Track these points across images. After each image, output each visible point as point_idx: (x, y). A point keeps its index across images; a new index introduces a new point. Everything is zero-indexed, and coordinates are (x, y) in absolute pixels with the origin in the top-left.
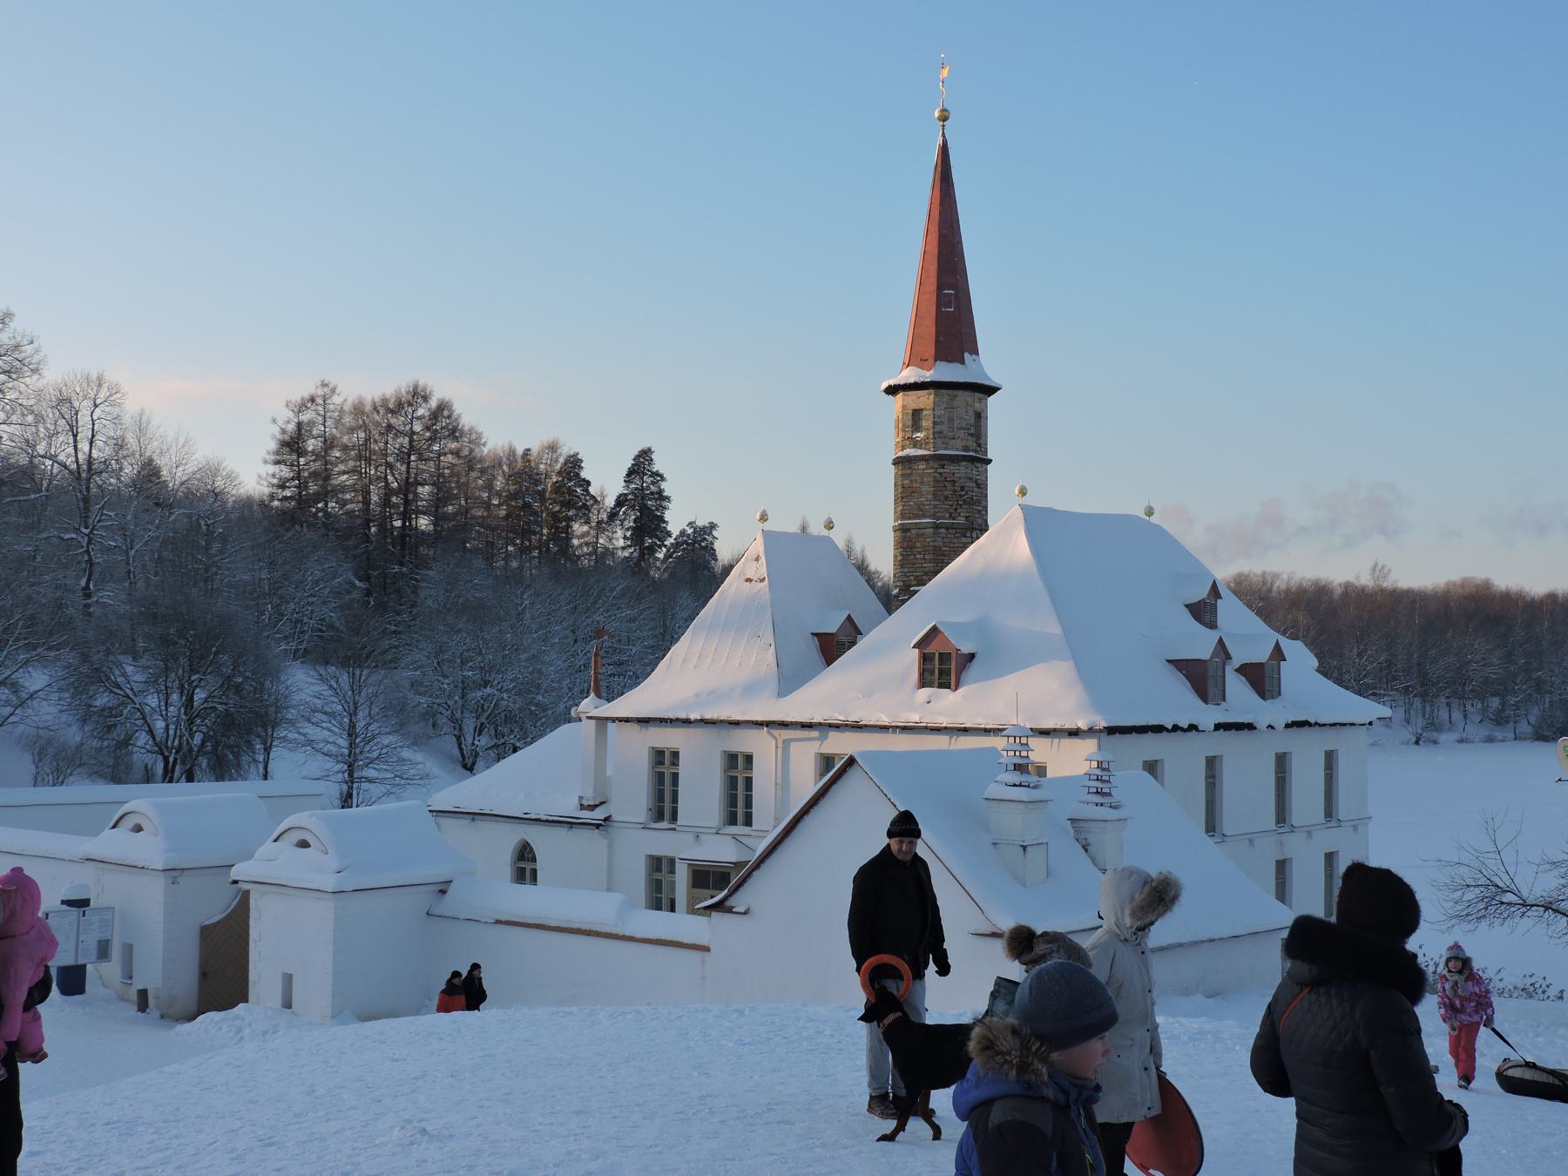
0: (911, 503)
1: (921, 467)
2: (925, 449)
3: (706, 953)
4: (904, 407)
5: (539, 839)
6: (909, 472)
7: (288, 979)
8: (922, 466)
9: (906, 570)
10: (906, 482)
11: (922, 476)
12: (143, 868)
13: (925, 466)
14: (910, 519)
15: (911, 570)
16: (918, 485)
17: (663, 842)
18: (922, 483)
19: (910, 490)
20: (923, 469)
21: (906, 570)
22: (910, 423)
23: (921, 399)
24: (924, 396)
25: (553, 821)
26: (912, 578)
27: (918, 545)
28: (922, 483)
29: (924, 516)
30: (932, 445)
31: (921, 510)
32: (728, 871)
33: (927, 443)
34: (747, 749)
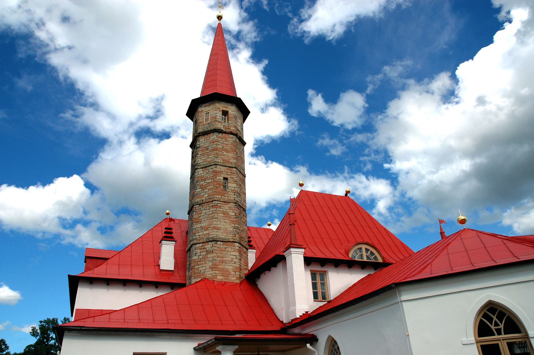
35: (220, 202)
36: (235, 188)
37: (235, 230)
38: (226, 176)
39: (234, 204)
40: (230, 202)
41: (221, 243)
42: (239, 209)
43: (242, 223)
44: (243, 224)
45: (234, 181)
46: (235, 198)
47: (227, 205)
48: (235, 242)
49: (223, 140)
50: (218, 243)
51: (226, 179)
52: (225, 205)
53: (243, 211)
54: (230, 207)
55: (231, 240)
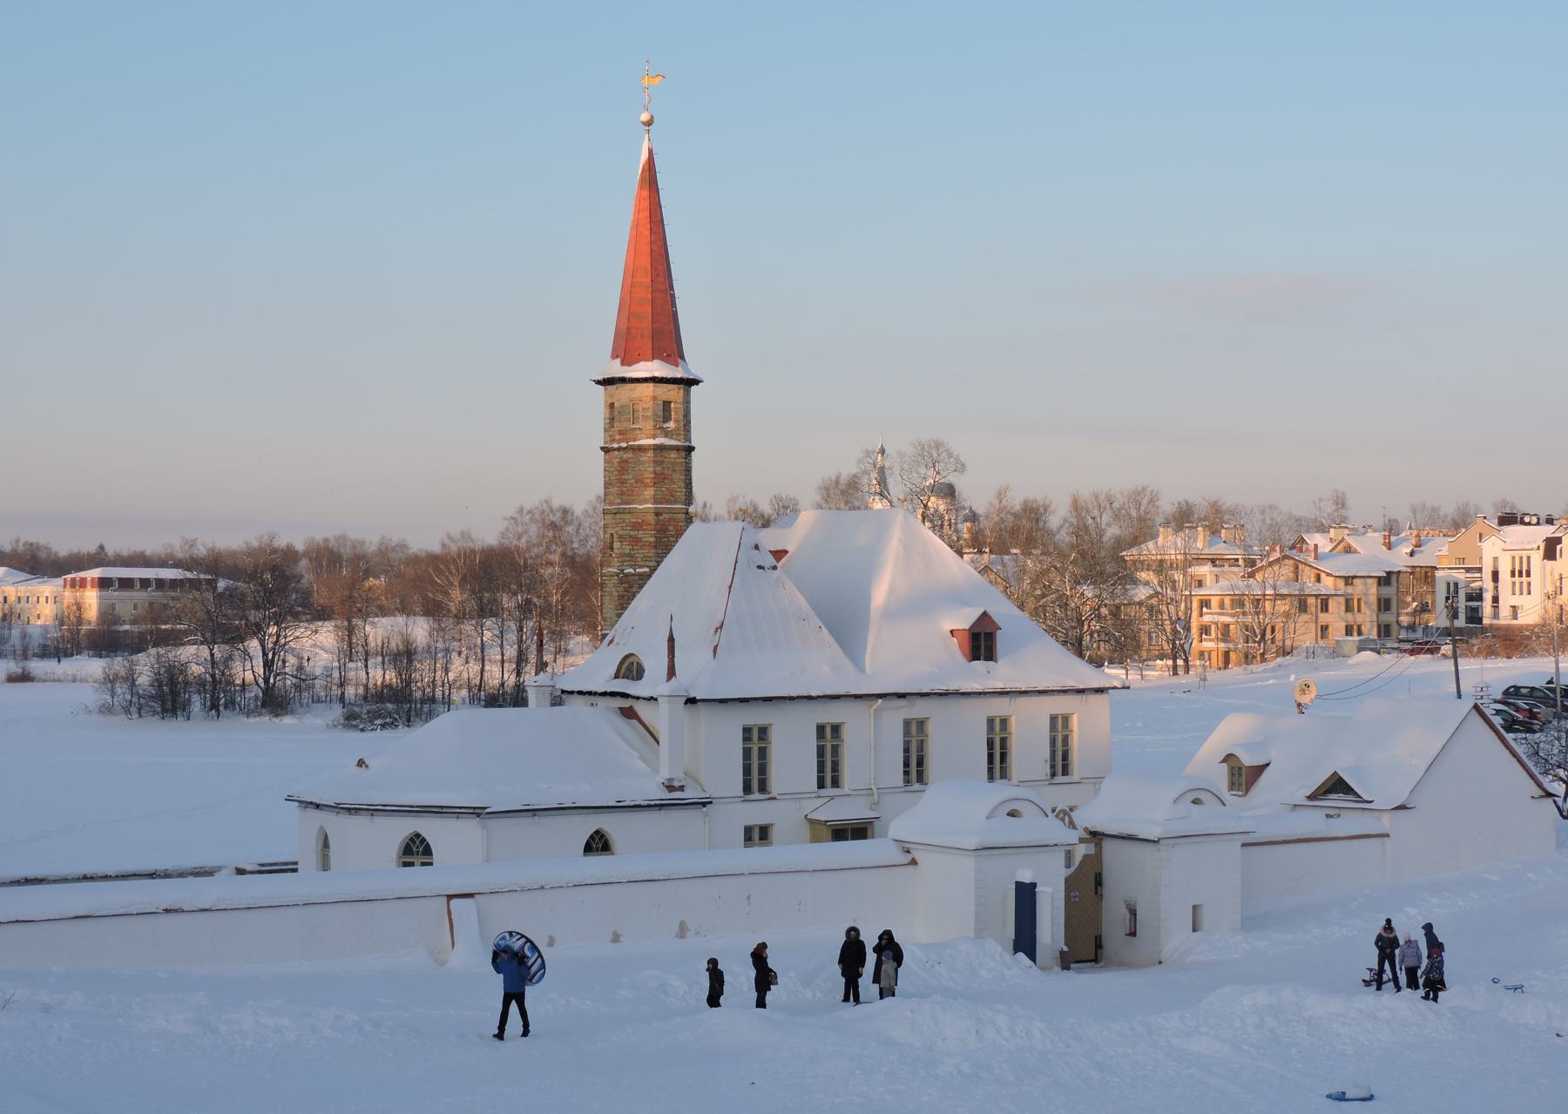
0: (663, 489)
1: (672, 456)
2: (676, 439)
3: (1386, 839)
4: (655, 398)
5: (612, 826)
6: (661, 459)
7: (1195, 908)
8: (673, 455)
9: (660, 551)
10: (658, 469)
11: (673, 464)
12: (1056, 845)
13: (676, 456)
14: (661, 504)
16: (670, 472)
17: (757, 812)
18: (674, 471)
19: (662, 477)
20: (676, 458)
21: (660, 551)
22: (661, 413)
23: (671, 392)
24: (674, 390)
25: (655, 805)
27: (671, 528)
28: (674, 471)
29: (676, 502)
30: (682, 437)
31: (673, 496)
32: (865, 825)
33: (678, 435)
34: (835, 720)
42: (625, 583)
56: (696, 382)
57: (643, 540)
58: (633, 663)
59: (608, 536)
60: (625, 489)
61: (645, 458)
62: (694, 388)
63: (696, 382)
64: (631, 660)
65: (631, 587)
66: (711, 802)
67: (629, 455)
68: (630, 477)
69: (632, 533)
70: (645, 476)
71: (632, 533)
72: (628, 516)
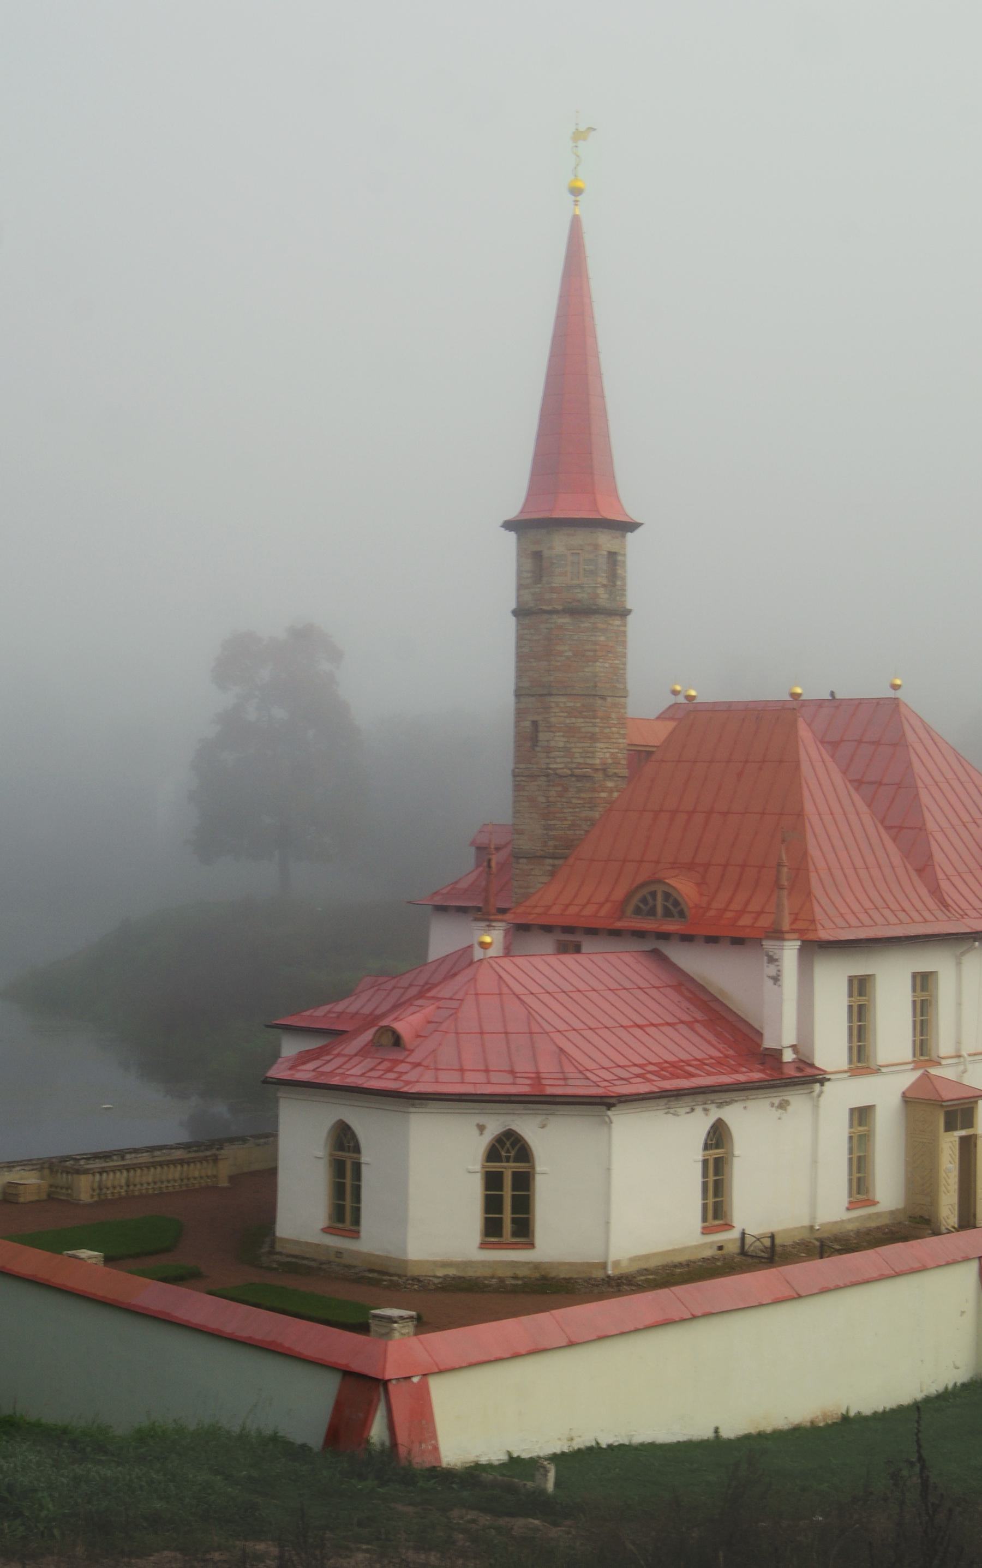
0: (607, 665)
15: (607, 745)
26: (608, 755)
27: (613, 716)
35: (523, 779)
36: (548, 741)
37: (545, 832)
38: (535, 718)
39: (544, 778)
40: (539, 776)
41: (525, 860)
43: (571, 810)
44: (577, 810)
45: (548, 725)
46: (548, 764)
47: (536, 783)
48: (546, 857)
49: (532, 631)
50: (521, 861)
51: (535, 723)
52: (531, 782)
53: (578, 781)
54: (538, 785)
55: (538, 854)
56: (632, 526)
57: (583, 730)
58: (653, 894)
59: (528, 724)
60: (559, 664)
61: (587, 625)
62: (629, 535)
63: (632, 526)
64: (652, 888)
65: (566, 789)
66: (829, 1080)
67: (564, 620)
68: (566, 648)
69: (568, 721)
70: (587, 647)
71: (568, 721)
72: (563, 699)
